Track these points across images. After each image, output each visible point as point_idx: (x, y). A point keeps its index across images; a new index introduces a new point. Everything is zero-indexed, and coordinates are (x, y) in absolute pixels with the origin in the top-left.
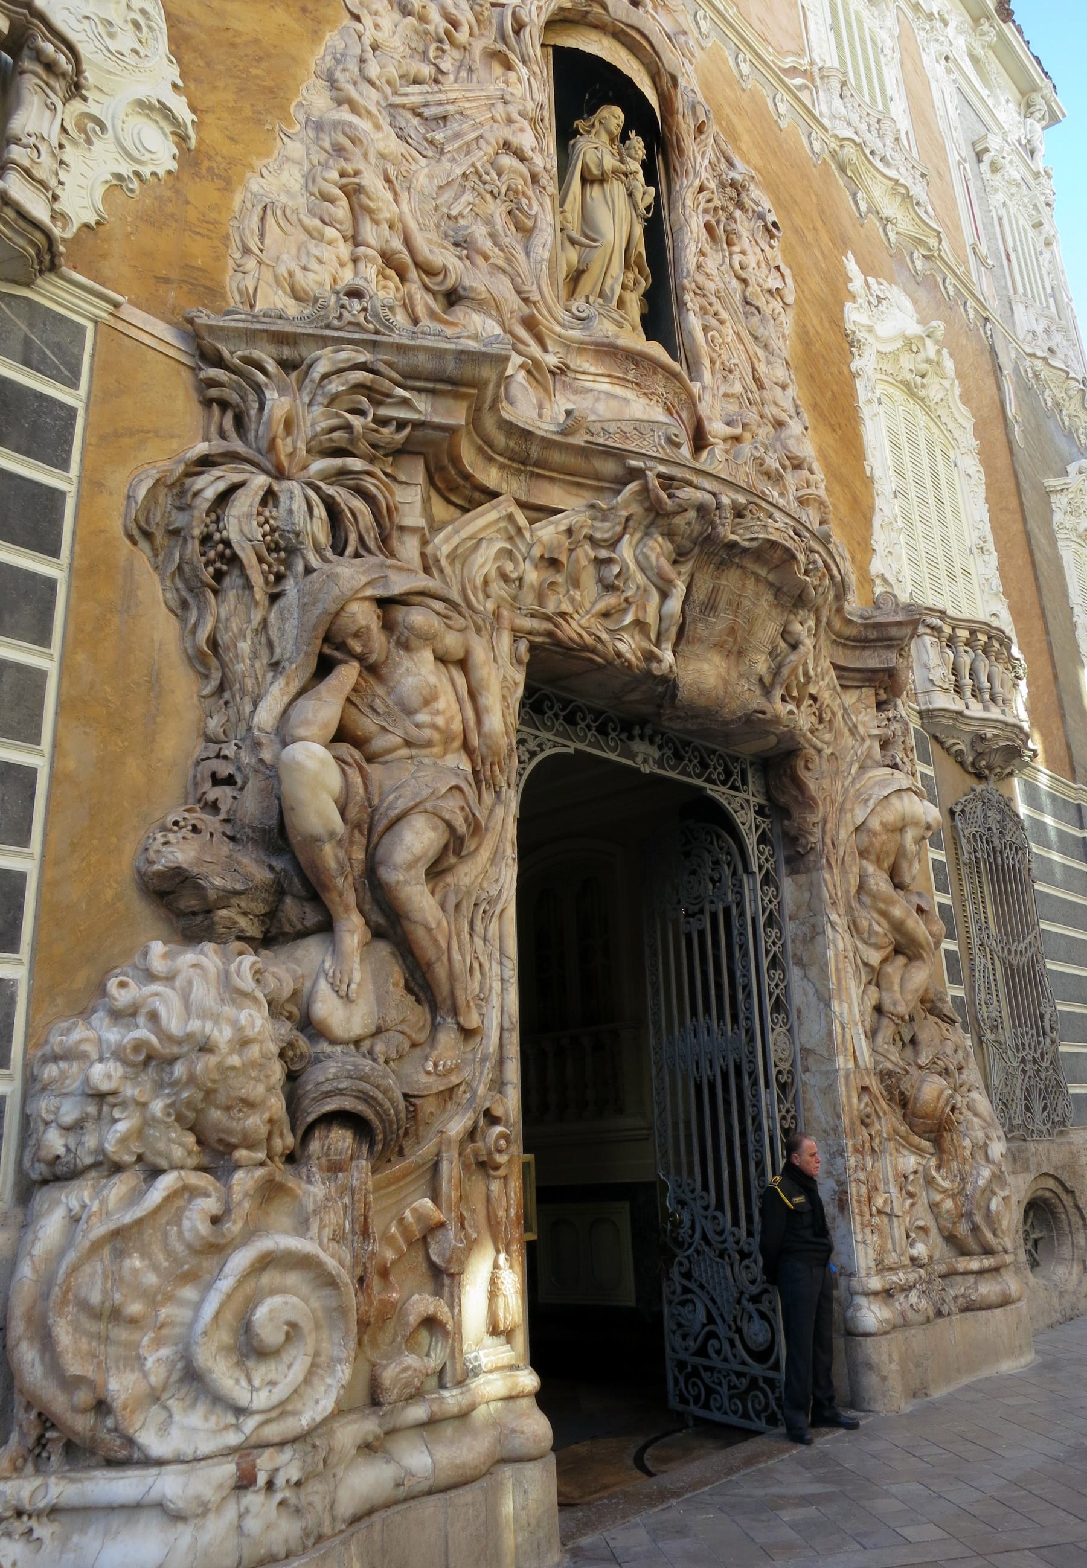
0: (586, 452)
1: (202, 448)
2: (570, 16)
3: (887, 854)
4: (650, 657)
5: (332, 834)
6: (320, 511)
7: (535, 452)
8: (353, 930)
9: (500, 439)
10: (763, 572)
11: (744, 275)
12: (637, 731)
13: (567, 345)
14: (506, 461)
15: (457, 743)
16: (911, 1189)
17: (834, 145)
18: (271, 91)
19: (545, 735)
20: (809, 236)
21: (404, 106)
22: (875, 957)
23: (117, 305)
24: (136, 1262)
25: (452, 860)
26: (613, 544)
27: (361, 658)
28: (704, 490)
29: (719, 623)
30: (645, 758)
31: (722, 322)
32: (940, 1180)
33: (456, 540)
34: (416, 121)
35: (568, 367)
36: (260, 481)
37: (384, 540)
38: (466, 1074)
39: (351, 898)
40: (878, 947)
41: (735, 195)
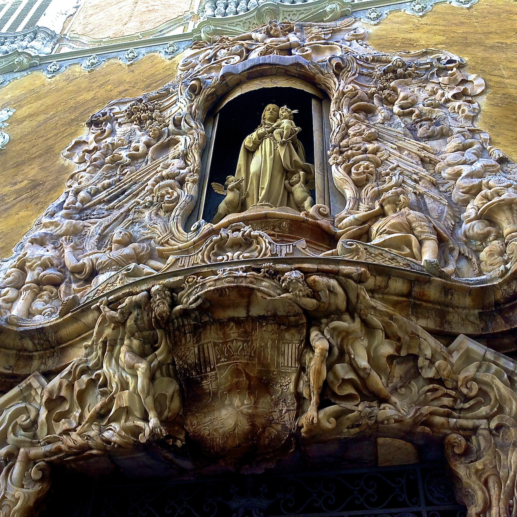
7: (52, 337)
10: (241, 313)
14: (41, 352)
28: (142, 291)
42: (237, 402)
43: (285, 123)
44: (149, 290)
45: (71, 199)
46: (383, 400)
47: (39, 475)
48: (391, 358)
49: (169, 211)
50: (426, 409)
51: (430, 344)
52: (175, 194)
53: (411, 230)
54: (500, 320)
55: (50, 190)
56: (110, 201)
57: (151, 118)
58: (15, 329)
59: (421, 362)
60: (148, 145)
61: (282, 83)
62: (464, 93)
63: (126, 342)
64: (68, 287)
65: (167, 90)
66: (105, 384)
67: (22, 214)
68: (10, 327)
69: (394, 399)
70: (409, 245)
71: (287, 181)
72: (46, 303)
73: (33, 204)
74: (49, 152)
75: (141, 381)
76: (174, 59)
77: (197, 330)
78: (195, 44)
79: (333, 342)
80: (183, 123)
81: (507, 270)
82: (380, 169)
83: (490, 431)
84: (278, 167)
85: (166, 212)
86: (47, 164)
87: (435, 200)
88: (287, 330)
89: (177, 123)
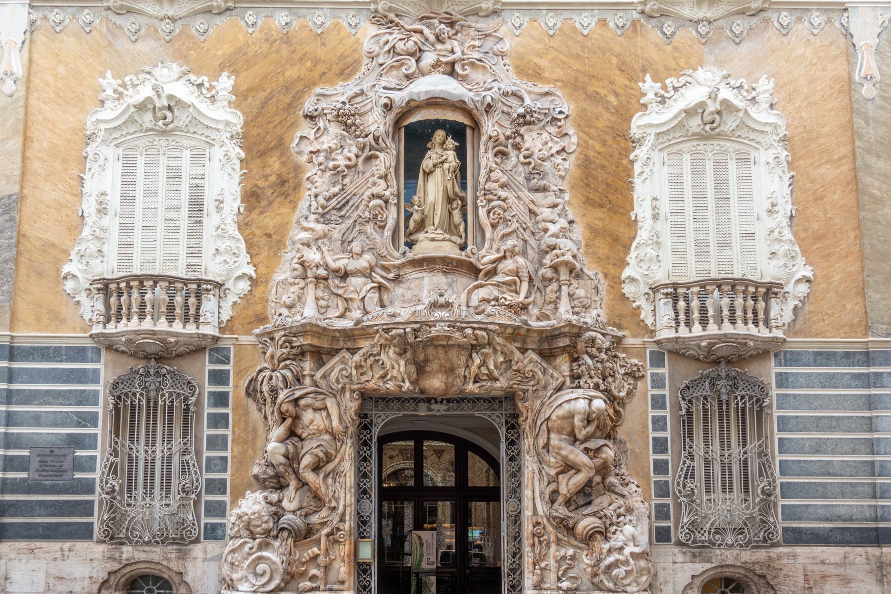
4: (400, 387)
5: (281, 464)
6: (281, 379)
7: (350, 334)
8: (293, 484)
9: (338, 335)
10: (445, 343)
11: (527, 160)
12: (433, 401)
13: (398, 267)
16: (569, 562)
18: (280, 241)
19: (388, 413)
20: (602, 92)
24: (236, 555)
25: (321, 464)
26: (379, 354)
27: (290, 416)
29: (435, 366)
30: (439, 409)
32: (585, 560)
34: (334, 212)
36: (267, 373)
37: (298, 380)
38: (330, 518)
39: (293, 476)
41: (522, 121)
43: (451, 155)
46: (497, 380)
49: (383, 227)
50: (512, 382)
55: (295, 189)
56: (340, 209)
59: (513, 363)
60: (357, 156)
62: (563, 150)
65: (362, 90)
70: (515, 283)
75: (402, 369)
76: (357, 36)
78: (374, 17)
80: (381, 140)
82: (506, 214)
84: (445, 196)
85: (380, 227)
86: (283, 159)
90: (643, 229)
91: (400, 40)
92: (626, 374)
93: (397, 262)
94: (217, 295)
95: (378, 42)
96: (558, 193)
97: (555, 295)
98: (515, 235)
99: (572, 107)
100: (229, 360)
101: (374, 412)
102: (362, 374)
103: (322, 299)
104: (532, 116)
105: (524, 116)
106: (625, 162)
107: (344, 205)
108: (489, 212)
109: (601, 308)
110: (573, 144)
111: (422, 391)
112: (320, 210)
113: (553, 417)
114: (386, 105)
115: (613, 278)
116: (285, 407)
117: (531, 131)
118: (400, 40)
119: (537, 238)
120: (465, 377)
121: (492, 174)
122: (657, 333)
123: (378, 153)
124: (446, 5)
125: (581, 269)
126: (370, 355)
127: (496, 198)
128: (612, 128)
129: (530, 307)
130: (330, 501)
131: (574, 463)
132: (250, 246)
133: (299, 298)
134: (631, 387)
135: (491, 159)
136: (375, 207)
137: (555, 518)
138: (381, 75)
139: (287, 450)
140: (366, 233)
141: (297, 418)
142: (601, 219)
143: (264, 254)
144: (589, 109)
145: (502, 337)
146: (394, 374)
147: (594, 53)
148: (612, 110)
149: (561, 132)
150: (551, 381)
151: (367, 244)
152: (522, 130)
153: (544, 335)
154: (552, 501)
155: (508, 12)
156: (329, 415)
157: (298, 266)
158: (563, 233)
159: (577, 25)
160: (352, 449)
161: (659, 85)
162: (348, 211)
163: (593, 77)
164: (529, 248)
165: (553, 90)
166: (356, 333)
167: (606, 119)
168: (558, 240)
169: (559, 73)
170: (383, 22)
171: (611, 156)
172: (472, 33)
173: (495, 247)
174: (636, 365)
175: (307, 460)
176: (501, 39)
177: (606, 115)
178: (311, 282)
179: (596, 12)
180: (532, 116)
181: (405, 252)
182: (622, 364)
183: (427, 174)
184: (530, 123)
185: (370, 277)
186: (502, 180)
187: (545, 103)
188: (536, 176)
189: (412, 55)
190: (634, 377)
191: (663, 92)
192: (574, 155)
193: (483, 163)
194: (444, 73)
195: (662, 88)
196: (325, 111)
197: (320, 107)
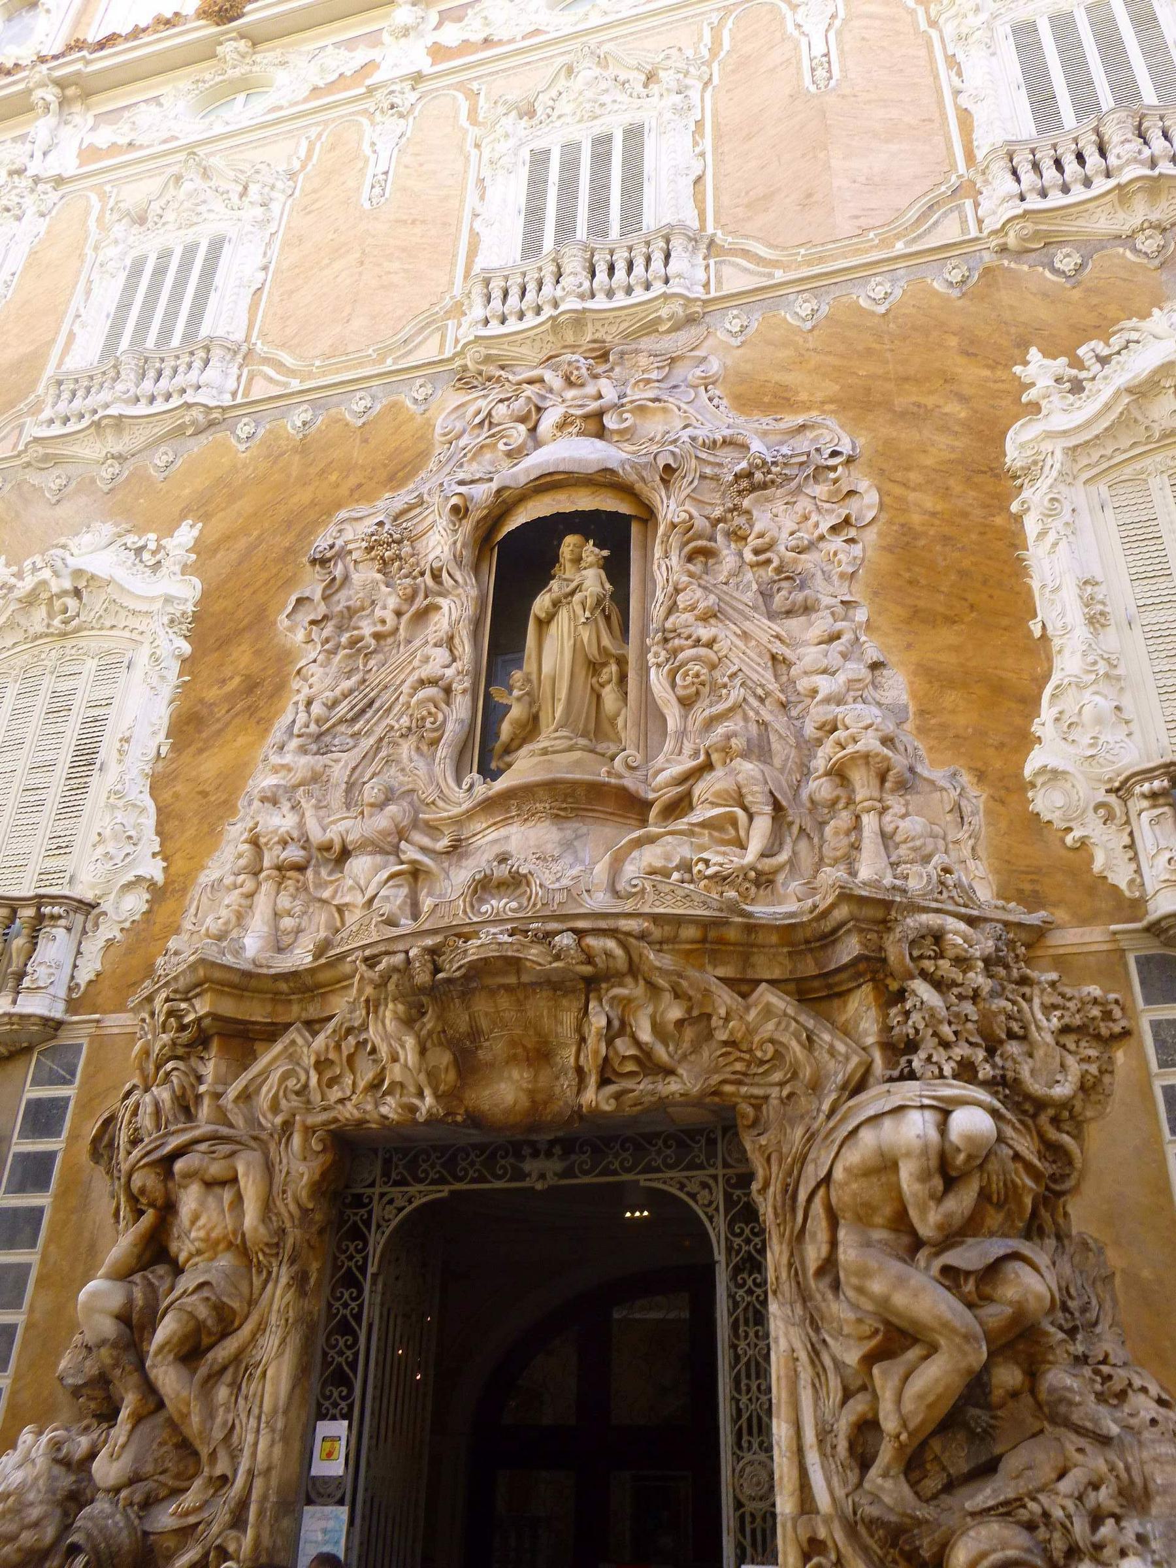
0: (330, 965)
1: (127, 1086)
2: (496, 512)
3: (867, 1205)
7: (309, 981)
9: (283, 986)
10: (512, 980)
11: (762, 557)
12: (526, 1151)
15: (222, 1246)
17: (994, 243)
18: (225, 802)
19: (412, 1190)
21: (334, 726)
22: (852, 1357)
23: (98, 1021)
27: (152, 1205)
30: (540, 1174)
31: (710, 645)
33: (244, 1083)
34: (342, 728)
35: (460, 840)
40: (861, 1339)
41: (744, 483)
42: (516, 1074)
44: (407, 952)
45: (302, 717)
46: (670, 1072)
47: (319, 1148)
48: (680, 1023)
49: (435, 743)
50: (716, 1078)
51: (725, 999)
52: (440, 717)
53: (740, 800)
54: (809, 960)
55: (271, 697)
56: (354, 719)
57: (399, 557)
58: (265, 971)
59: (715, 1022)
60: (399, 614)
61: (585, 501)
62: (847, 521)
63: (391, 1006)
64: (317, 873)
65: (420, 496)
66: (374, 1051)
67: (241, 740)
68: (260, 971)
69: (680, 1071)
70: (734, 822)
71: (594, 680)
72: (294, 897)
73: (254, 720)
74: (261, 619)
77: (466, 995)
79: (612, 1015)
80: (445, 575)
81: (815, 907)
82: (717, 674)
83: (781, 1098)
84: (580, 660)
87: (781, 736)
88: (564, 996)
89: (436, 577)
90: (1067, 652)
91: (501, 401)
92: (1066, 1030)
93: (456, 811)
94: (78, 927)
95: (463, 416)
96: (840, 609)
97: (845, 842)
98: (738, 717)
99: (861, 441)
100: (73, 1075)
101: (377, 1190)
102: (333, 1081)
103: (289, 914)
104: (769, 472)
105: (750, 475)
106: (999, 521)
107: (363, 711)
108: (673, 674)
109: (975, 857)
110: (869, 507)
111: (475, 1120)
112: (313, 728)
113: (839, 1174)
114: (455, 509)
115: (1001, 780)
116: (137, 1181)
117: (768, 500)
118: (501, 401)
119: (794, 713)
120: (579, 1070)
121: (680, 598)
122: (1151, 906)
123: (440, 600)
124: (590, 329)
125: (911, 769)
126: (349, 1031)
127: (690, 642)
128: (959, 462)
129: (780, 878)
130: (213, 1455)
131: (914, 1322)
132: (167, 821)
133: (240, 917)
134: (1093, 1069)
135: (676, 568)
136: (421, 703)
137: (872, 1524)
138: (461, 466)
139: (130, 1301)
140: (398, 762)
141: (168, 1209)
142: (956, 649)
143: (191, 832)
144: (903, 435)
145: (673, 952)
146: (393, 1075)
147: (905, 339)
148: (957, 428)
149: (838, 491)
150: (832, 1065)
151: (401, 784)
152: (746, 503)
153: (800, 935)
154: (863, 1461)
155: (718, 314)
156: (239, 1198)
157: (246, 846)
158: (855, 691)
159: (863, 302)
160: (289, 1296)
161: (1063, 360)
162: (368, 722)
163: (906, 379)
164: (773, 738)
165: (819, 420)
166: (324, 976)
167: (943, 447)
168: (841, 708)
169: (832, 388)
170: (476, 383)
171: (965, 515)
172: (643, 360)
173: (688, 748)
174: (1095, 1001)
175: (167, 1329)
176: (705, 359)
177: (943, 440)
178: (269, 877)
179: (902, 272)
180: (769, 472)
181: (472, 786)
182: (1048, 1000)
183: (543, 624)
184: (764, 486)
185: (396, 851)
186: (702, 605)
187: (803, 443)
188: (785, 584)
189: (523, 420)
190: (1098, 1037)
191: (1074, 372)
192: (874, 529)
193: (660, 579)
194: (578, 434)
195: (1070, 366)
196: (350, 547)
197: (339, 543)
